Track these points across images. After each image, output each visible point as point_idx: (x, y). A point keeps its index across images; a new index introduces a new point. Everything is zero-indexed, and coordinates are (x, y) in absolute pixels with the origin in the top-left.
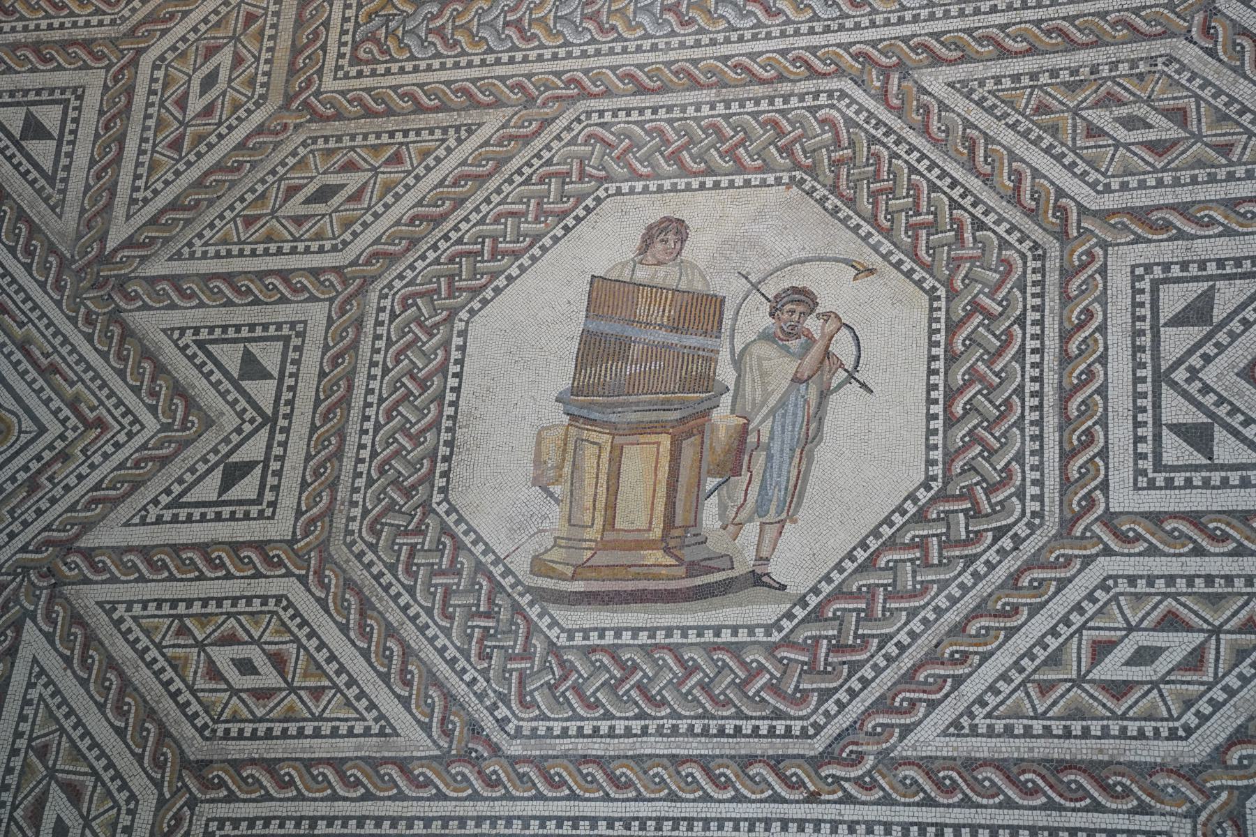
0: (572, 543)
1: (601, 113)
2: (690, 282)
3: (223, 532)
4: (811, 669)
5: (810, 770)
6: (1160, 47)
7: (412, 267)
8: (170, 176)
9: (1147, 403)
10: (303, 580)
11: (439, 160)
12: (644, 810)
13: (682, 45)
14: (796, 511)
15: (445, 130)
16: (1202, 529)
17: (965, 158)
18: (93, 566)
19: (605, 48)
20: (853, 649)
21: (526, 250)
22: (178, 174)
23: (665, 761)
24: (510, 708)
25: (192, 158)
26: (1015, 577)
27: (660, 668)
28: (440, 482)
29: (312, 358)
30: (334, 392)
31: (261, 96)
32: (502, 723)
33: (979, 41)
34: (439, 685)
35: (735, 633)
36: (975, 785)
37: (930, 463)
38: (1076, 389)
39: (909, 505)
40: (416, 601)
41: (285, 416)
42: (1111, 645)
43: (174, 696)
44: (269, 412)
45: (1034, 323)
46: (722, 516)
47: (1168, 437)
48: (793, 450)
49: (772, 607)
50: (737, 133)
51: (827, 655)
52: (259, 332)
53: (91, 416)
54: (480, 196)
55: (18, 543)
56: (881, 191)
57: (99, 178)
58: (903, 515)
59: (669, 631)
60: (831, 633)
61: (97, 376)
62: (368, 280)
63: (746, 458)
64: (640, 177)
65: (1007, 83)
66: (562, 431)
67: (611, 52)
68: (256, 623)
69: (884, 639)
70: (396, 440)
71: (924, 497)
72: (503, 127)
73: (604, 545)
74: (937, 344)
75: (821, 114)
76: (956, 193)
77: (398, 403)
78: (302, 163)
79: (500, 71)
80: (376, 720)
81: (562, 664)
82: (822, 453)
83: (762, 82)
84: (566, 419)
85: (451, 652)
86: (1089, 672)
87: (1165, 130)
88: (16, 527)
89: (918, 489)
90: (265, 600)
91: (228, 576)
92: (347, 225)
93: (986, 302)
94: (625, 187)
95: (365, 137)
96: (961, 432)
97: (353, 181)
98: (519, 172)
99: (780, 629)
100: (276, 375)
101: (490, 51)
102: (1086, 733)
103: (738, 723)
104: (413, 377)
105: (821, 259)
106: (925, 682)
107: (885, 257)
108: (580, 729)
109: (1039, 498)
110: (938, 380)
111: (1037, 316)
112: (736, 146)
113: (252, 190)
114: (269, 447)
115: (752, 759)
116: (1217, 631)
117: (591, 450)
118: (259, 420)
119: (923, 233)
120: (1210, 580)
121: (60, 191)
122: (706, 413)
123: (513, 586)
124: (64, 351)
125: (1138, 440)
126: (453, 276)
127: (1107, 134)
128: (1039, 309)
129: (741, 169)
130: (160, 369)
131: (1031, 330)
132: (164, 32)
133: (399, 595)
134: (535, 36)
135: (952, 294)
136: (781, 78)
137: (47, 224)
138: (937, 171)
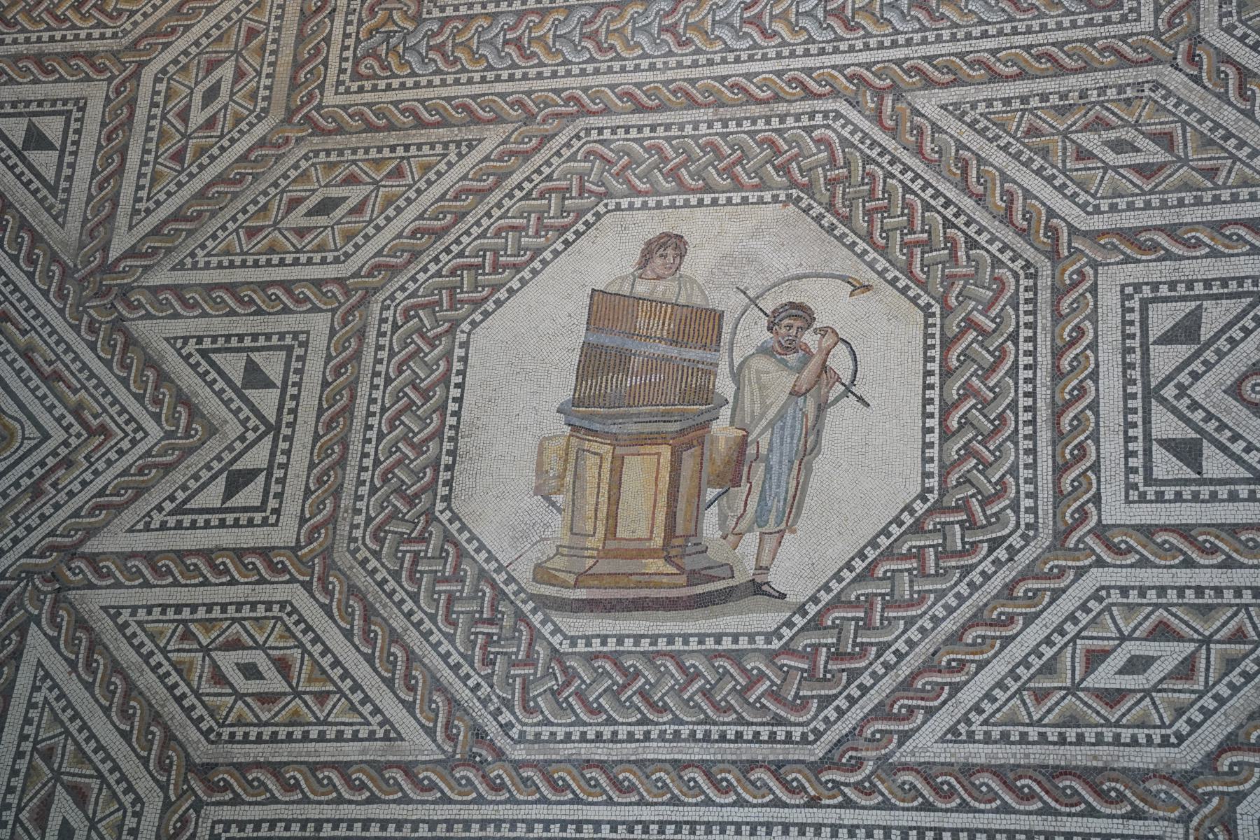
0: (574, 552)
1: (600, 130)
2: (689, 296)
3: (227, 538)
4: (810, 676)
5: (810, 775)
6: (1147, 73)
7: (413, 279)
8: (172, 188)
9: (1138, 418)
10: (307, 586)
11: (439, 175)
12: (646, 813)
13: (680, 65)
14: (795, 522)
15: (446, 145)
16: (1192, 541)
18: (97, 571)
19: (604, 67)
20: (852, 657)
21: (528, 262)
22: (180, 185)
23: (668, 766)
24: (513, 713)
25: (194, 169)
26: (1010, 587)
27: (663, 674)
28: (443, 491)
29: (315, 368)
30: (336, 402)
31: (263, 110)
32: (506, 727)
33: (971, 65)
34: (443, 690)
35: (736, 641)
36: (973, 790)
37: (926, 475)
38: (1068, 404)
40: (419, 607)
41: (289, 425)
42: (1104, 654)
43: (179, 700)
44: (273, 420)
45: (1027, 340)
47: (1158, 452)
48: (791, 462)
49: (772, 615)
52: (262, 342)
53: (95, 423)
54: (481, 210)
55: (22, 548)
56: (876, 210)
57: (101, 188)
58: (900, 526)
59: (671, 639)
61: (100, 383)
63: (746, 469)
64: (639, 193)
65: (998, 106)
66: (563, 442)
67: (610, 70)
68: (261, 628)
70: (399, 449)
71: (920, 508)
72: (503, 143)
73: (606, 554)
74: (932, 359)
75: (816, 134)
76: (949, 212)
77: (401, 412)
78: (304, 176)
79: (500, 88)
80: (381, 725)
81: (565, 670)
82: (821, 465)
84: (568, 429)
85: (455, 658)
86: (1083, 680)
87: (1153, 153)
88: (20, 532)
89: (914, 500)
90: (269, 605)
91: (233, 582)
92: (349, 237)
93: (980, 318)
94: (625, 203)
95: (367, 151)
96: (956, 446)
97: (354, 194)
98: (520, 187)
99: (780, 637)
100: (279, 384)
101: (490, 68)
102: (1080, 740)
103: (740, 728)
104: (415, 388)
105: (818, 276)
106: (923, 690)
107: (880, 274)
108: (583, 734)
109: (1033, 510)
110: (934, 394)
111: (1030, 333)
112: (734, 164)
113: (255, 202)
114: (273, 454)
115: (753, 764)
116: (1207, 641)
118: (262, 428)
119: (918, 251)
120: (1199, 591)
121: (62, 201)
122: (706, 425)
123: (515, 594)
124: (68, 358)
125: (1129, 454)
127: (1096, 157)
128: (1031, 326)
129: (738, 186)
130: (163, 377)
131: (1023, 346)
132: (166, 46)
133: (402, 601)
134: (534, 54)
135: (947, 311)
136: (777, 98)
137: (49, 233)
138: (930, 191)
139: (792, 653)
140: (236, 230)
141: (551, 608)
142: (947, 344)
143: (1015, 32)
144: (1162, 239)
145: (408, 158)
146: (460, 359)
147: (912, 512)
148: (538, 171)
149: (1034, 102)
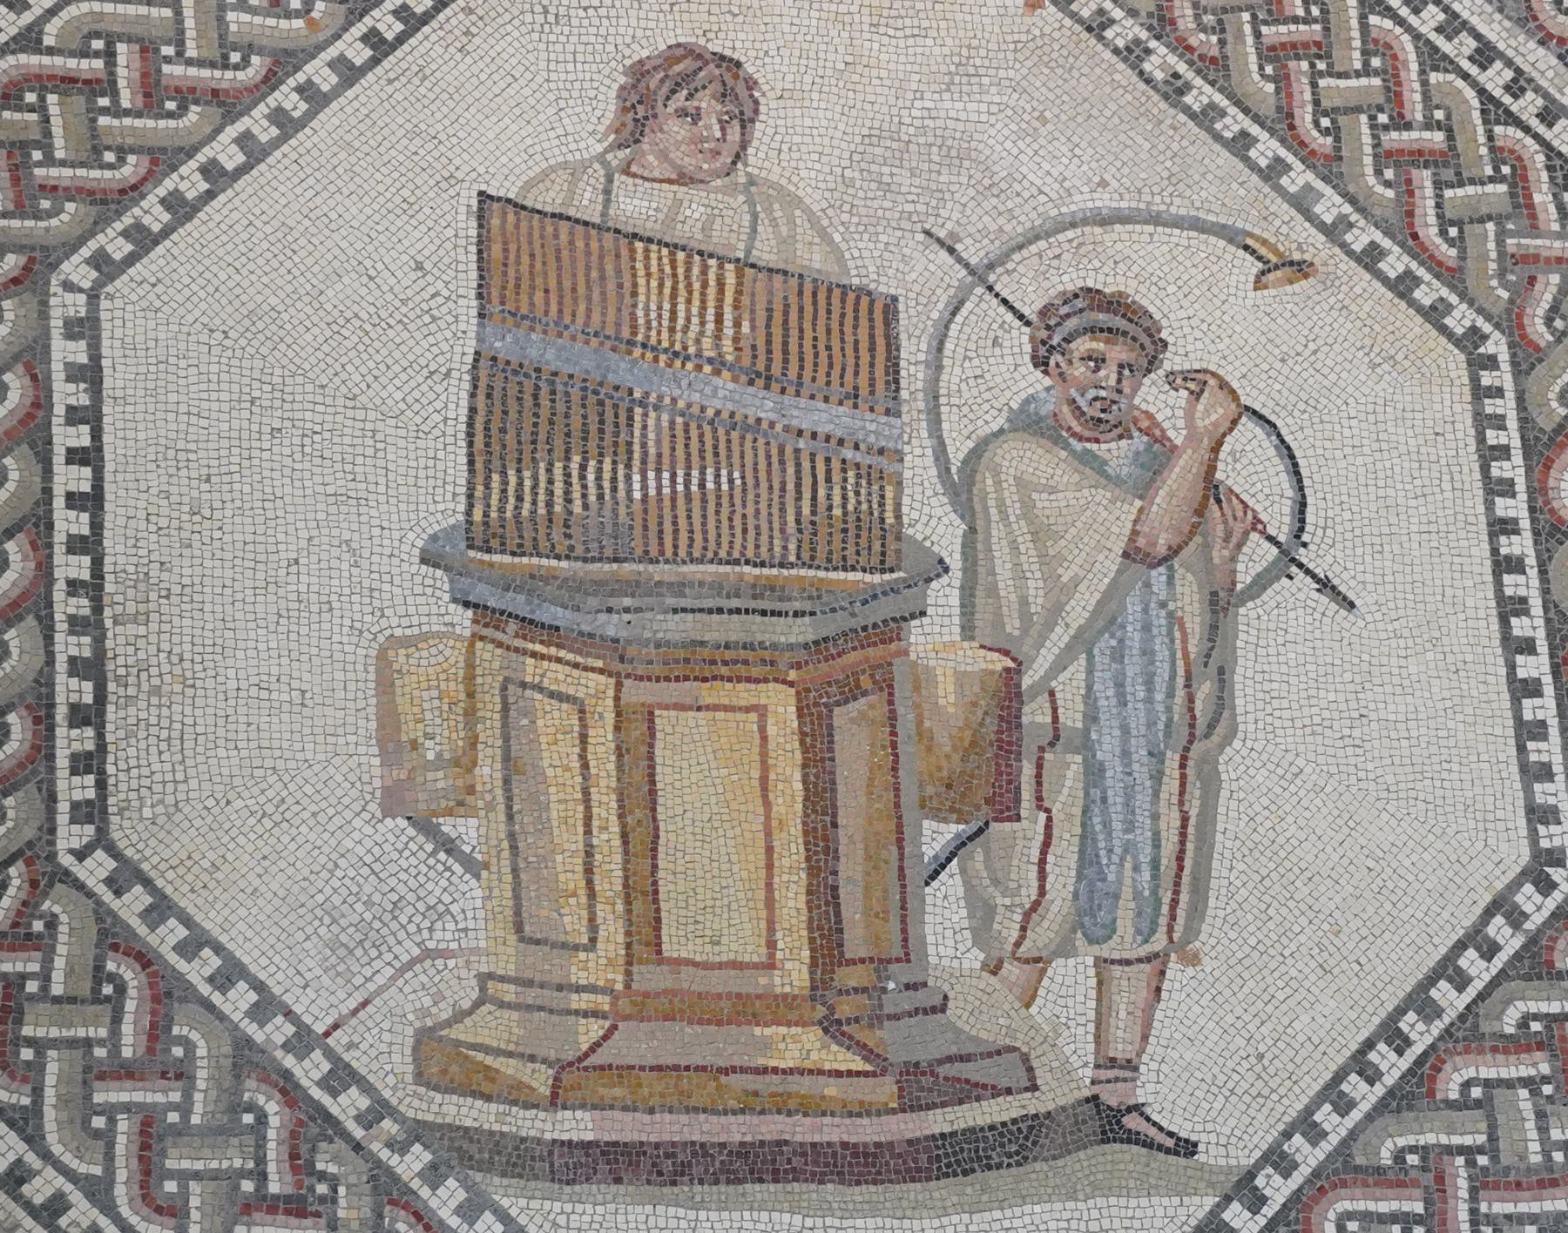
0: (540, 996)
14: (1192, 932)
28: (74, 789)
39: (1498, 928)
40: (47, 1156)
46: (982, 931)
48: (1156, 755)
63: (1028, 770)
66: (455, 655)
73: (637, 1007)
74: (1506, 488)
76: (1495, 78)
82: (1242, 767)
84: (463, 619)
89: (1515, 885)
105: (1156, 220)
107: (1334, 232)
117: (553, 719)
122: (891, 631)
123: (368, 1120)
141: (486, 1167)
147: (1516, 918)
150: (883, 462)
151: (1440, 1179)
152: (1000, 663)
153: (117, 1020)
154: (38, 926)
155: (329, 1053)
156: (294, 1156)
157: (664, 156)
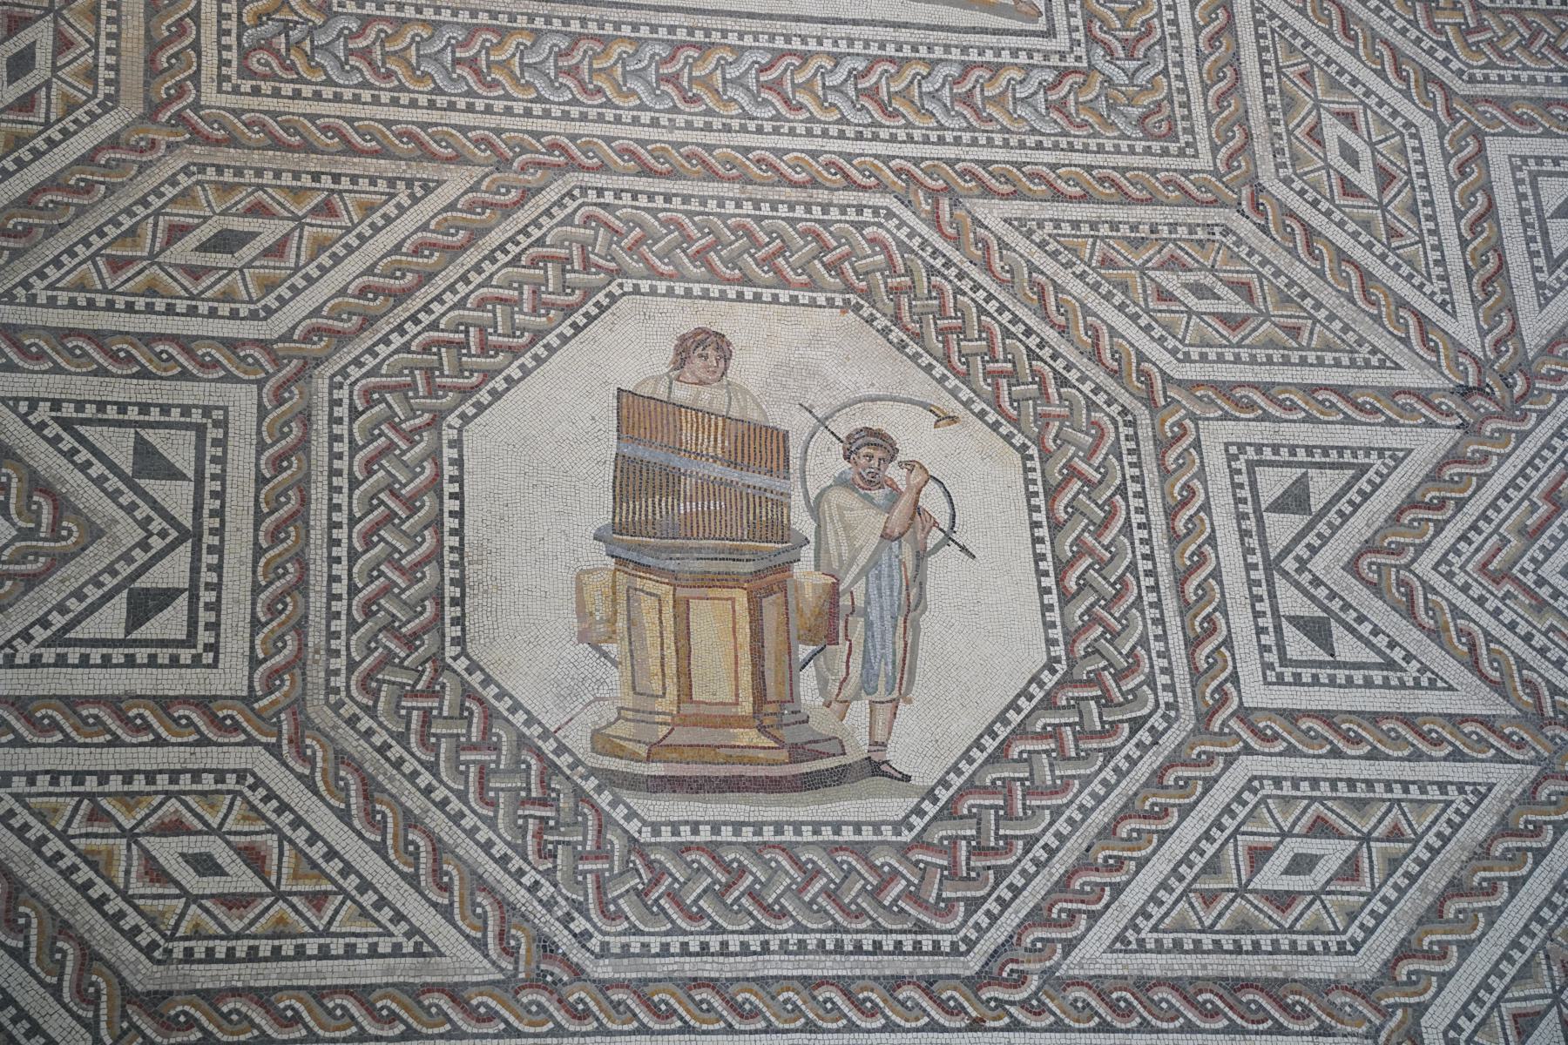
0: (643, 716)
1: (600, 192)
3: (141, 681)
4: (951, 874)
6: (1215, 215)
7: (371, 351)
9: (1262, 591)
10: (274, 750)
11: (388, 220)
14: (909, 690)
15: (391, 182)
16: (1336, 729)
17: (1036, 304)
20: (995, 851)
21: (528, 346)
23: (796, 984)
24: (589, 920)
26: (1159, 774)
28: (452, 632)
29: (242, 461)
32: (582, 938)
34: (490, 891)
35: (858, 831)
37: (1051, 643)
39: (1034, 688)
40: (441, 782)
43: (99, 904)
48: (894, 618)
50: (773, 240)
51: (968, 859)
54: (453, 272)
59: (779, 828)
60: (968, 832)
62: (310, 364)
63: (842, 624)
64: (662, 276)
65: (1067, 229)
66: (608, 577)
68: (212, 806)
69: (1031, 842)
70: (381, 574)
71: (1050, 680)
72: (471, 189)
74: (1037, 509)
76: (1033, 342)
78: (186, 196)
81: (650, 865)
82: (930, 624)
83: (794, 184)
85: (499, 849)
89: (1041, 671)
90: (220, 776)
92: (269, 286)
93: (1083, 466)
94: (645, 286)
95: (278, 174)
97: (269, 231)
98: (502, 248)
99: (911, 828)
101: (438, 90)
102: (1256, 949)
103: (878, 937)
104: (394, 494)
105: (894, 399)
106: (1082, 891)
107: (967, 404)
108: (685, 945)
109: (1170, 687)
112: (775, 255)
114: (195, 570)
115: (898, 981)
117: (648, 603)
118: (174, 534)
120: (1352, 784)
122: (786, 567)
123: (572, 767)
125: (1260, 631)
126: (432, 369)
127: (1177, 299)
128: (1138, 479)
129: (785, 284)
135: (1045, 456)
136: (814, 183)
139: (928, 847)
140: (92, 258)
141: (620, 786)
142: (1052, 493)
143: (1071, 149)
144: (1257, 397)
145: (340, 192)
146: (452, 462)
147: (1041, 685)
148: (524, 231)
149: (1104, 230)
150: (782, 498)
151: (1010, 791)
152: (831, 580)
153: (470, 726)
154: (438, 688)
155: (556, 740)
156: (542, 782)
157: (693, 373)
